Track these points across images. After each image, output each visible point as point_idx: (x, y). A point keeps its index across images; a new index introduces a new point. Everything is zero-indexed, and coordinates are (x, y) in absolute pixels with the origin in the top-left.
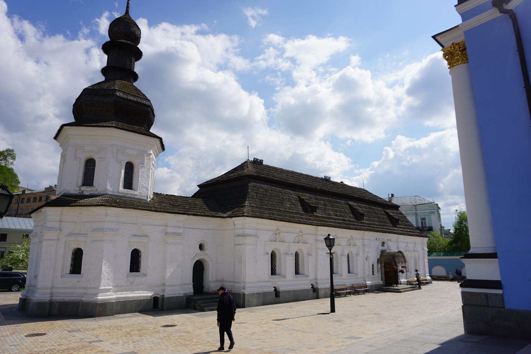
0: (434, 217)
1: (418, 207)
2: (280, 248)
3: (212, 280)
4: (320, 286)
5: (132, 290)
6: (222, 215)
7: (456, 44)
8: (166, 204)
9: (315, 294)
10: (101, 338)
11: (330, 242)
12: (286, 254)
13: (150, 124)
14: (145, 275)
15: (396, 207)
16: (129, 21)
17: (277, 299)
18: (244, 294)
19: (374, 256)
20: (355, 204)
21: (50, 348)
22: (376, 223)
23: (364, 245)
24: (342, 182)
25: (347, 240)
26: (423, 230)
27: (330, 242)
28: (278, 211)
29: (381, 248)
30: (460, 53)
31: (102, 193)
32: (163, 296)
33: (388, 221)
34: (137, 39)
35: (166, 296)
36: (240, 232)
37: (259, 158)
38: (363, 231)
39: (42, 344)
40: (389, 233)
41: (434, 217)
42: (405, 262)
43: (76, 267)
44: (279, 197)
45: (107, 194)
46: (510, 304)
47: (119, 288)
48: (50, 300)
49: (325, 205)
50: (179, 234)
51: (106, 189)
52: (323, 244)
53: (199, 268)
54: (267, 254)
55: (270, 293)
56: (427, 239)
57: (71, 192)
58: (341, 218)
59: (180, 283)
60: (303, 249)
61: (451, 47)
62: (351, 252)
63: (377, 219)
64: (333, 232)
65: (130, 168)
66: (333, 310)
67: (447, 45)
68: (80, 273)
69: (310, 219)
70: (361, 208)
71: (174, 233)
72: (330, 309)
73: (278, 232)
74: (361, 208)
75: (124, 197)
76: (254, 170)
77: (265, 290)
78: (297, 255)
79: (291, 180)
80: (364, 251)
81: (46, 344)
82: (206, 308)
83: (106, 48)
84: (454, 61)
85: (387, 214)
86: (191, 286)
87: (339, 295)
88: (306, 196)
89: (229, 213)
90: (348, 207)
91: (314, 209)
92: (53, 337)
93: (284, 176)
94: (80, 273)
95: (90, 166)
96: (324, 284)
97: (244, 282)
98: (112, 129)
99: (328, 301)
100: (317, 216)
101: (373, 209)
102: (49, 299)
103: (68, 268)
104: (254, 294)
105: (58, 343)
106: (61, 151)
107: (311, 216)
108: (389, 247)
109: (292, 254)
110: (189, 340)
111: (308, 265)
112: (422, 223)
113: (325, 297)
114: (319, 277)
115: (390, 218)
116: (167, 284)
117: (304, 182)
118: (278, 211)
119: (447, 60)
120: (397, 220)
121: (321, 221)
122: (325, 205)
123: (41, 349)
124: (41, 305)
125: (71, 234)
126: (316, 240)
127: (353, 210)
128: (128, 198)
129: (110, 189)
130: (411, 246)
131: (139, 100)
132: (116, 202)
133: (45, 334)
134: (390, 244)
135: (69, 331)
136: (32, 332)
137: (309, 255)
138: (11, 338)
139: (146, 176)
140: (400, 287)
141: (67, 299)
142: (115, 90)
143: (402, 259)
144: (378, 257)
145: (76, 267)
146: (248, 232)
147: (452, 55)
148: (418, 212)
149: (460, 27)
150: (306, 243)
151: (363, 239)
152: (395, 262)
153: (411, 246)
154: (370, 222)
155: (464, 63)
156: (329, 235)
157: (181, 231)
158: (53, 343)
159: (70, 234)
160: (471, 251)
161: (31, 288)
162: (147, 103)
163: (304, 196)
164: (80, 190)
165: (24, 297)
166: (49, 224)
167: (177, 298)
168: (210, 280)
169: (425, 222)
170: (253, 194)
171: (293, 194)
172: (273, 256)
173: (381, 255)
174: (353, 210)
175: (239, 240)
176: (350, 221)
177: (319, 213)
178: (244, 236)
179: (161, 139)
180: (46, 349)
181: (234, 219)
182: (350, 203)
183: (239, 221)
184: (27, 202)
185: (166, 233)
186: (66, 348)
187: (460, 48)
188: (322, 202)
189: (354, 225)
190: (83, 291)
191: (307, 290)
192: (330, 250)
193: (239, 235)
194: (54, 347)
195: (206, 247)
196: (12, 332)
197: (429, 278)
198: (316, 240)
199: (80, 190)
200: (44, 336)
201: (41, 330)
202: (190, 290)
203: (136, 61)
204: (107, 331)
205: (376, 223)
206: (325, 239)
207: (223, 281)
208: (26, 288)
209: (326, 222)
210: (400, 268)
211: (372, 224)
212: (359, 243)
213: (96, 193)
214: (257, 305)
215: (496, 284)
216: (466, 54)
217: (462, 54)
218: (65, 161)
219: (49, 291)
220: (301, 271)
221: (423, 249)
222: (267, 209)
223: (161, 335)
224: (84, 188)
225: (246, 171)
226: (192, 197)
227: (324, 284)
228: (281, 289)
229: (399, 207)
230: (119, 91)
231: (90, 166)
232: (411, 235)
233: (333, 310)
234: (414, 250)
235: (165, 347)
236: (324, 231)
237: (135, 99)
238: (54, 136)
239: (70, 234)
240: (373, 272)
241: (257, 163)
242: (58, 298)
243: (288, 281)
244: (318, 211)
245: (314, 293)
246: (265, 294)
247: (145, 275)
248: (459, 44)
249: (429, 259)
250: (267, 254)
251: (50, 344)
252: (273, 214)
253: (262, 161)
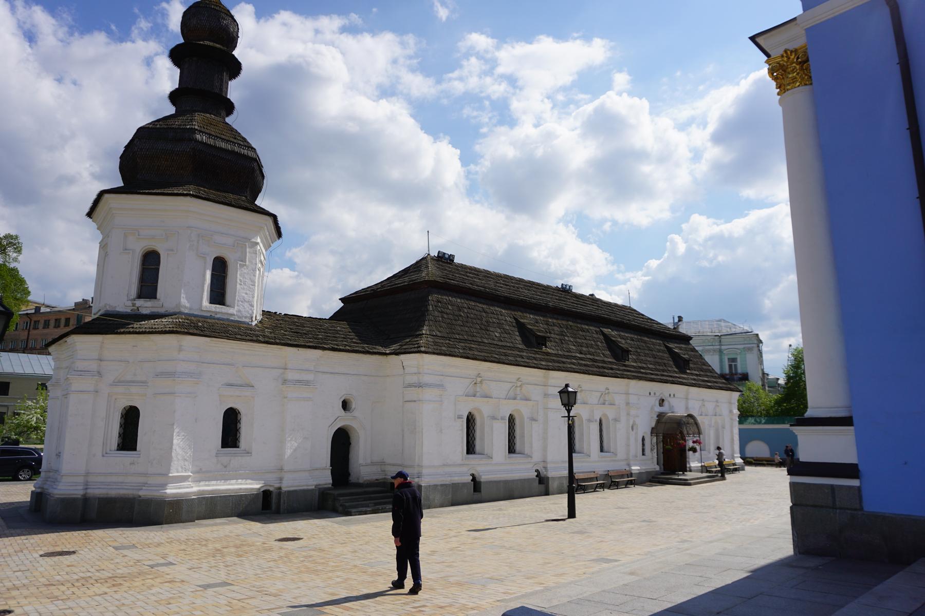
0: (751, 358)
1: (724, 339)
2: (483, 409)
3: (366, 463)
4: (550, 474)
5: (226, 479)
6: (382, 350)
7: (792, 52)
8: (285, 331)
9: (542, 487)
10: (171, 559)
11: (568, 398)
12: (494, 418)
13: (256, 190)
14: (248, 453)
15: (686, 339)
16: (218, 8)
17: (477, 496)
18: (420, 487)
19: (645, 424)
20: (614, 333)
21: (82, 575)
22: (651, 366)
23: (628, 404)
24: (592, 295)
25: (599, 394)
26: (732, 379)
27: (568, 398)
28: (479, 343)
29: (658, 409)
30: (798, 67)
31: (172, 311)
32: (280, 488)
33: (671, 363)
34: (232, 40)
35: (284, 489)
36: (413, 379)
37: (449, 252)
38: (626, 380)
39: (68, 569)
40: (673, 383)
41: (751, 358)
42: (699, 433)
43: (128, 438)
44: (481, 320)
45: (180, 313)
46: (871, 505)
47: (202, 474)
48: (84, 495)
49: (562, 334)
50: (307, 383)
51: (179, 305)
52: (557, 403)
53: (342, 441)
54: (460, 417)
55: (464, 485)
56: (739, 393)
57: (118, 309)
58: (589, 356)
59: (309, 467)
60: (523, 410)
61: (782, 56)
62: (605, 415)
63: (652, 359)
64: (575, 381)
65: (220, 268)
66: (572, 514)
67: (776, 53)
68: (135, 449)
69: (535, 359)
70: (624, 339)
71: (299, 381)
72: (567, 513)
73: (479, 379)
74: (624, 339)
75: (211, 317)
76: (438, 273)
77: (457, 479)
78: (511, 420)
79: (504, 291)
80: (628, 414)
81: (75, 570)
82: (353, 510)
83: (176, 55)
84: (786, 81)
85: (670, 350)
86: (329, 472)
87: (584, 489)
88: (528, 319)
89: (395, 347)
90: (602, 337)
91: (541, 341)
92: (88, 556)
93: (491, 284)
94: (135, 449)
96: (558, 471)
97: (420, 466)
98: (188, 198)
99: (564, 499)
100: (548, 354)
101: (645, 342)
102: (82, 492)
103: (114, 439)
104: (436, 485)
105: (97, 568)
106: (101, 237)
107: (536, 353)
108: (671, 407)
109: (503, 418)
110: (323, 563)
111: (531, 437)
112: (730, 366)
113: (561, 492)
114: (549, 459)
115: (675, 357)
116: (286, 468)
117: (525, 294)
118: (479, 343)
119: (775, 79)
120: (687, 362)
121: (554, 361)
122: (562, 334)
123: (67, 577)
124: (68, 502)
125: (120, 382)
126: (546, 395)
127: (611, 344)
128: (218, 319)
129: (185, 303)
130: (710, 407)
131: (236, 149)
132: (197, 327)
133: (74, 552)
134: (673, 401)
135: (116, 548)
136: (51, 550)
137: (533, 419)
138: (15, 558)
139: (248, 282)
140: (689, 475)
141: (113, 493)
142: (193, 131)
143: (694, 428)
144: (653, 425)
145: (128, 438)
146: (426, 379)
147: (784, 71)
148: (723, 347)
149: (798, 21)
150: (527, 400)
151: (627, 394)
152: (681, 433)
153: (710, 407)
154: (640, 365)
155: (806, 85)
156: (567, 386)
157: (310, 377)
158: (89, 567)
159: (117, 383)
160: (809, 413)
161: (51, 474)
162: (250, 154)
163: (524, 318)
164: (134, 305)
165: (39, 490)
166: (80, 365)
167: (305, 492)
168: (361, 461)
169: (736, 366)
170: (436, 313)
171: (506, 315)
172: (470, 421)
173: (658, 422)
174: (611, 344)
175: (412, 393)
176: (604, 362)
177: (550, 348)
178: (420, 386)
179: (274, 217)
180: (76, 577)
181: (402, 357)
182: (606, 330)
183: (410, 360)
184: (44, 328)
185: (285, 382)
186: (110, 575)
187: (798, 58)
188: (556, 328)
189: (612, 369)
190: (142, 480)
191: (528, 480)
192: (569, 411)
193: (410, 386)
194: (89, 574)
195: (353, 406)
196: (17, 548)
197: (739, 461)
198: (546, 395)
199: (134, 305)
200: (73, 556)
201: (68, 546)
202: (325, 478)
203: (230, 79)
204: (183, 547)
205: (651, 366)
206: (560, 392)
207: (382, 463)
208: (42, 474)
209: (564, 363)
210: (690, 444)
211: (643, 368)
212: (619, 400)
213: (162, 311)
214: (442, 506)
215: (850, 471)
216: (808, 69)
217: (802, 69)
218: (106, 255)
219: (81, 480)
220: (518, 447)
221: (731, 411)
222: (460, 340)
223: (274, 555)
224: (140, 303)
225: (423, 275)
226: (331, 318)
227: (558, 471)
228: (484, 478)
229: (690, 338)
230: (200, 131)
232: (710, 387)
233: (572, 514)
234: (715, 413)
235: (280, 575)
236: (559, 379)
237: (229, 147)
238: (87, 210)
239: (117, 383)
240: (643, 450)
241: (444, 260)
242: (97, 491)
243: (495, 464)
244: (548, 344)
245: (541, 485)
246: (455, 487)
247: (248, 453)
248: (796, 51)
249: (740, 430)
250: (460, 417)
251: (84, 569)
252: (470, 349)
253: (453, 256)
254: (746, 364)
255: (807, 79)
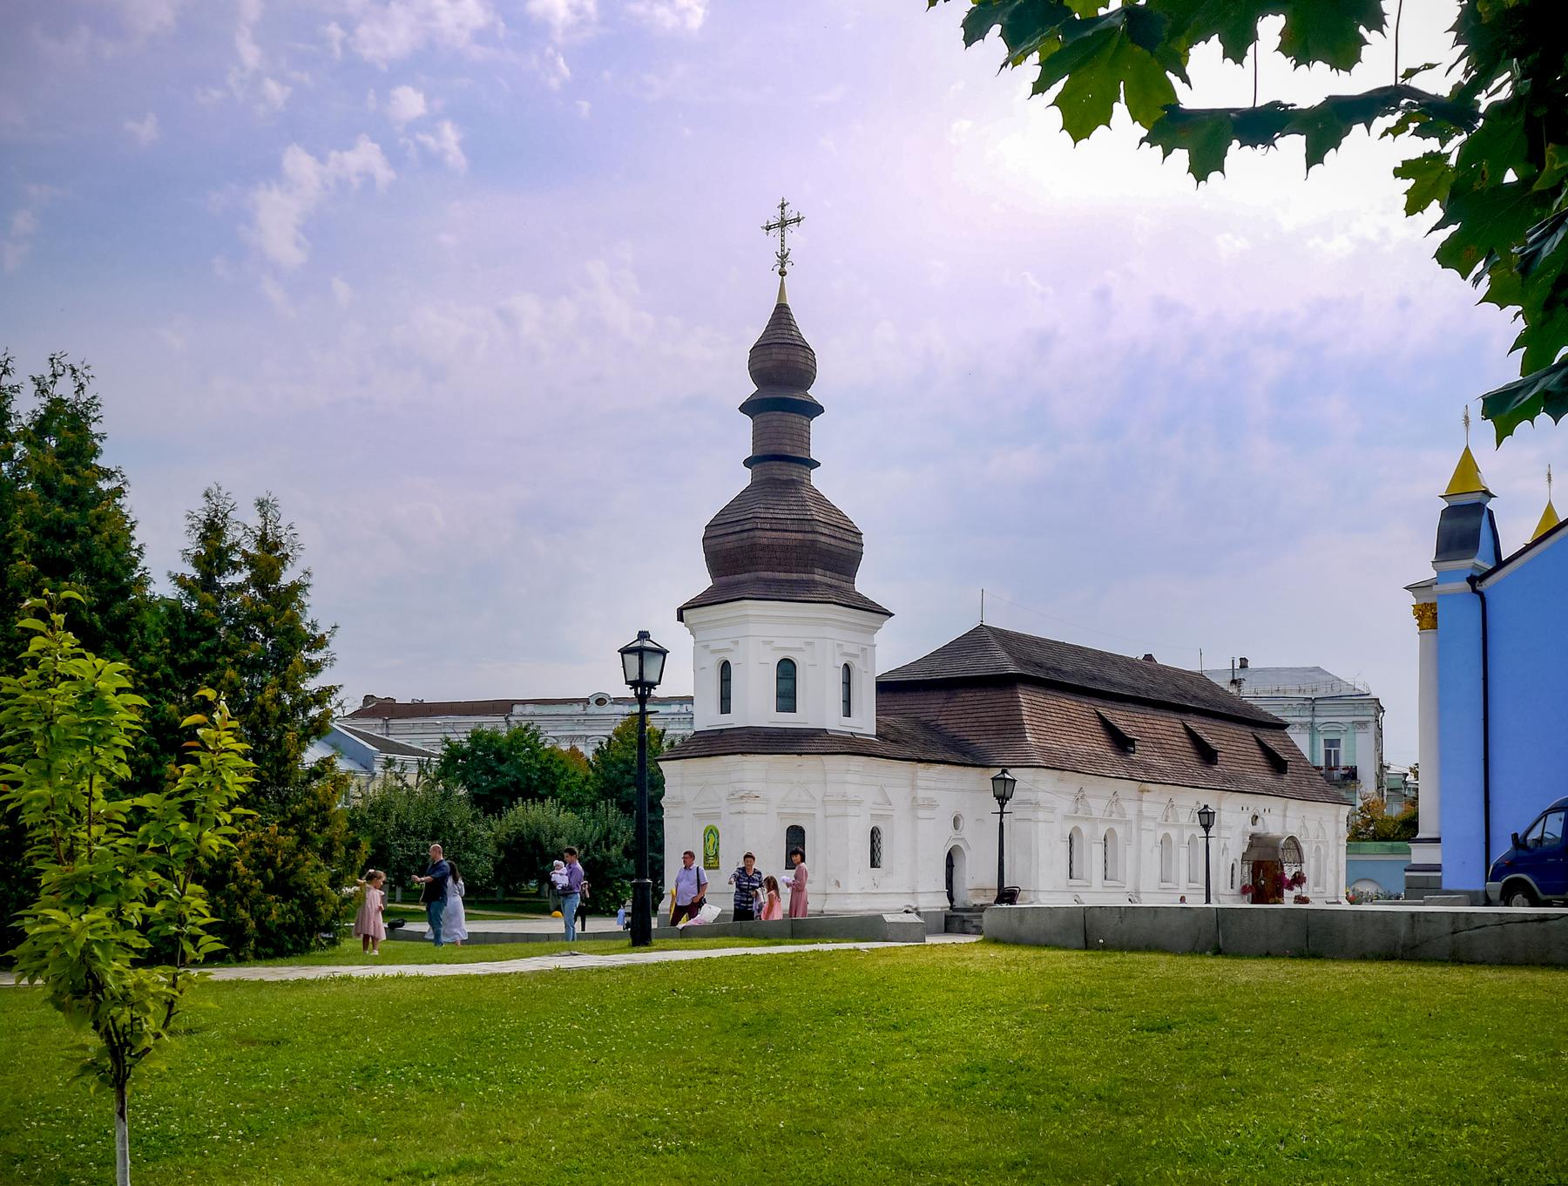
11: (1207, 819)
24: (1149, 658)
26: (1337, 780)
27: (1207, 819)
29: (1252, 829)
41: (1364, 740)
70: (1211, 733)
74: (1211, 733)
95: (787, 670)
112: (1328, 753)
134: (1267, 817)
143: (1295, 854)
148: (1317, 720)
153: (1312, 826)
173: (1251, 846)
215: (1437, 868)
231: (787, 670)
254: (1356, 752)
255: (1435, 627)
